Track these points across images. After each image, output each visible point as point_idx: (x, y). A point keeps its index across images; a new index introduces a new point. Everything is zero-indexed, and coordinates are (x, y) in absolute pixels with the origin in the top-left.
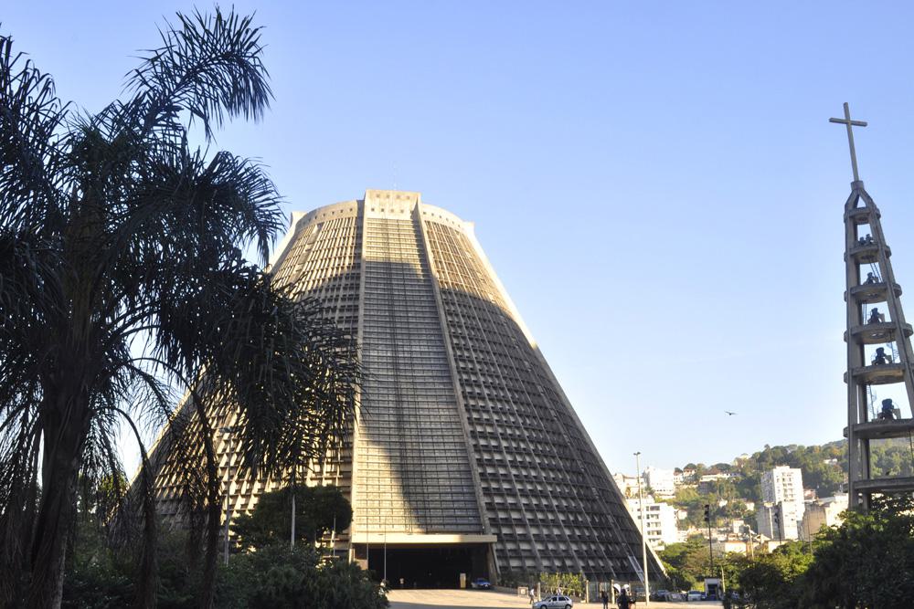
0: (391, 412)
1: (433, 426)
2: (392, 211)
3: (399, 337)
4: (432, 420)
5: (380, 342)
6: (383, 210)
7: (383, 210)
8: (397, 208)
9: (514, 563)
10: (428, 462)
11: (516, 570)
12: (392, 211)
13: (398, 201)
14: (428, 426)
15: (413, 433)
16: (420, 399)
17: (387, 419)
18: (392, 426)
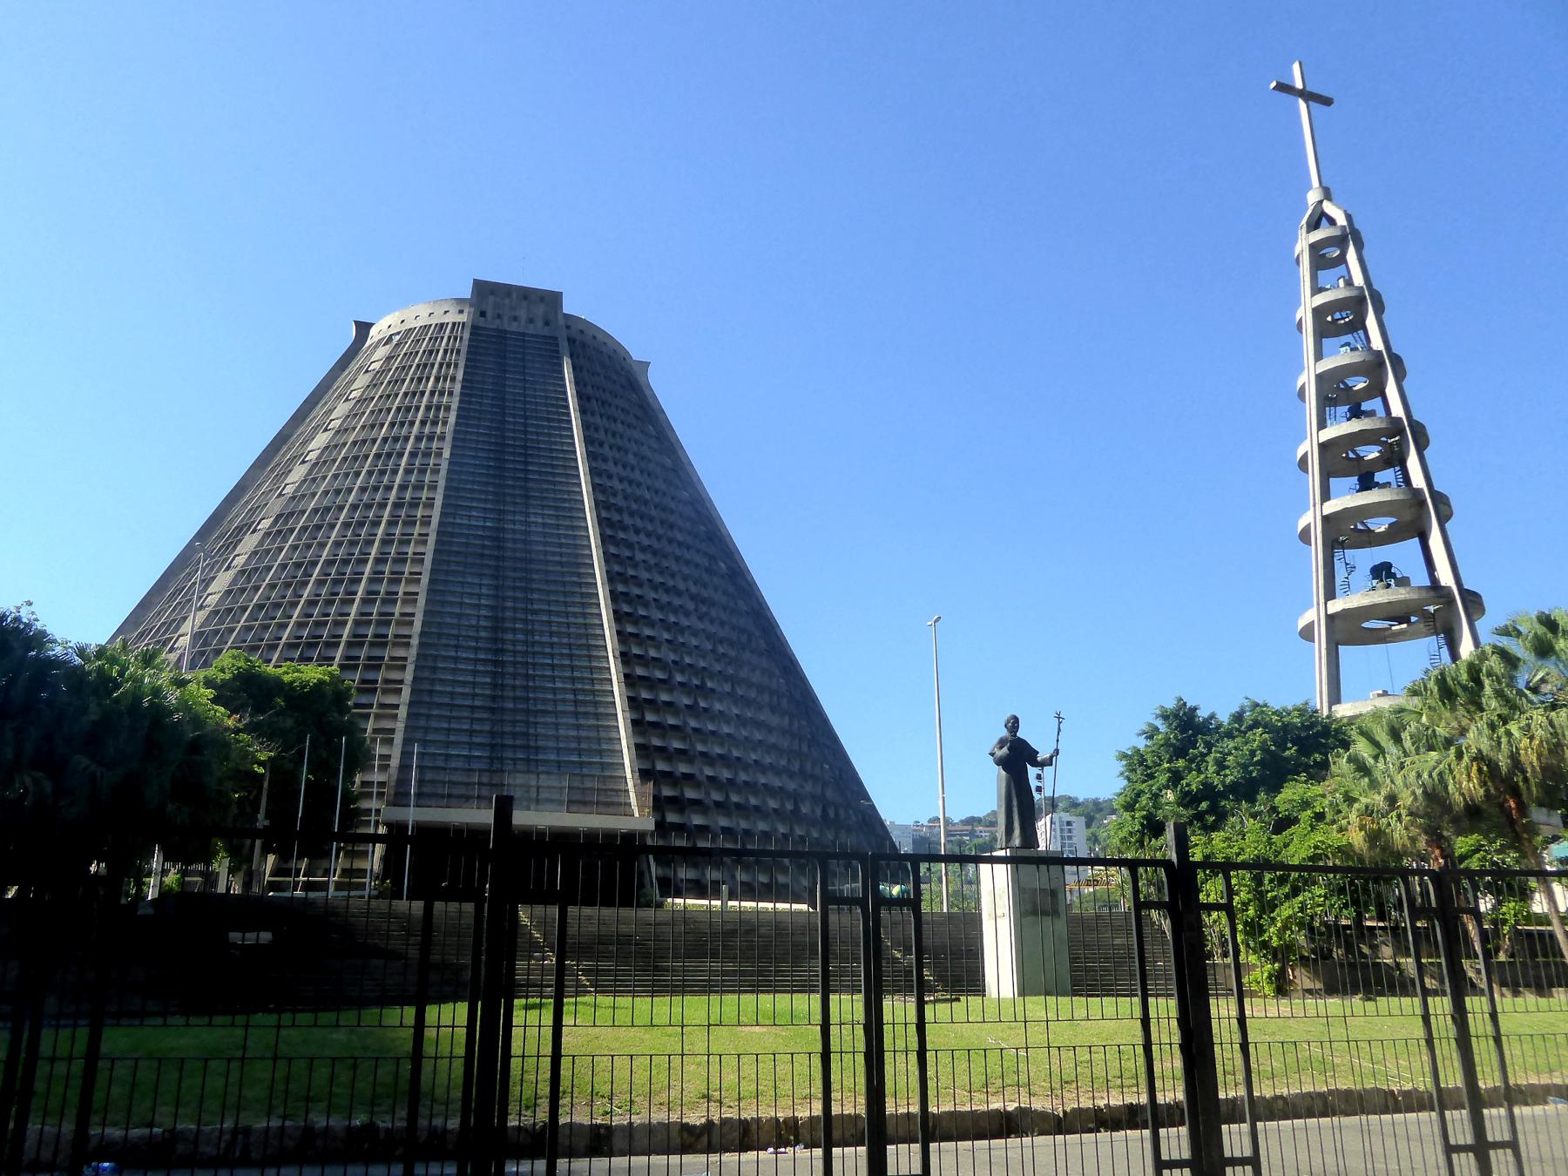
0: (483, 612)
1: (555, 640)
2: (515, 319)
4: (554, 629)
5: (474, 504)
6: (499, 316)
7: (499, 316)
8: (522, 314)
10: (541, 695)
12: (515, 319)
13: (525, 303)
14: (546, 639)
15: (519, 648)
16: (536, 596)
17: (474, 622)
18: (483, 634)
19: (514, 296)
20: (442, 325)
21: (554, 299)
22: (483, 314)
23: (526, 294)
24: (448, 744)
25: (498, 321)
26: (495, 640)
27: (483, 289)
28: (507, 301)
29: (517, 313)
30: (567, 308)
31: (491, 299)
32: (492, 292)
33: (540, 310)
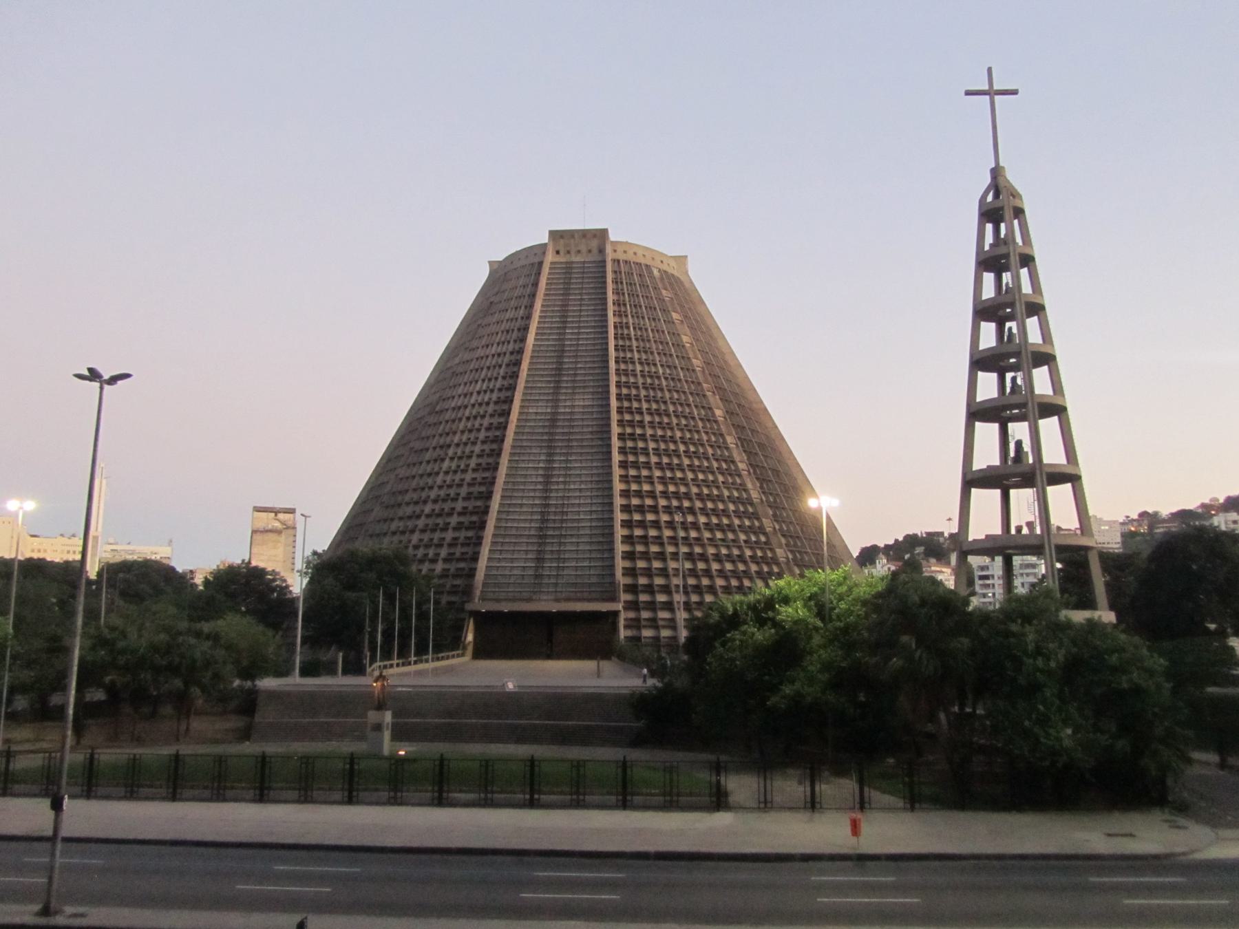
2: (579, 252)
3: (564, 391)
6: (569, 252)
7: (569, 252)
8: (583, 248)
9: (647, 633)
11: (647, 640)
12: (579, 252)
13: (584, 240)
19: (576, 236)
20: (532, 264)
21: (602, 234)
22: (558, 252)
23: (585, 234)
24: (512, 560)
25: (568, 256)
26: (546, 491)
27: (555, 235)
28: (572, 241)
29: (579, 248)
30: (613, 237)
31: (562, 241)
32: (562, 237)
33: (594, 244)
